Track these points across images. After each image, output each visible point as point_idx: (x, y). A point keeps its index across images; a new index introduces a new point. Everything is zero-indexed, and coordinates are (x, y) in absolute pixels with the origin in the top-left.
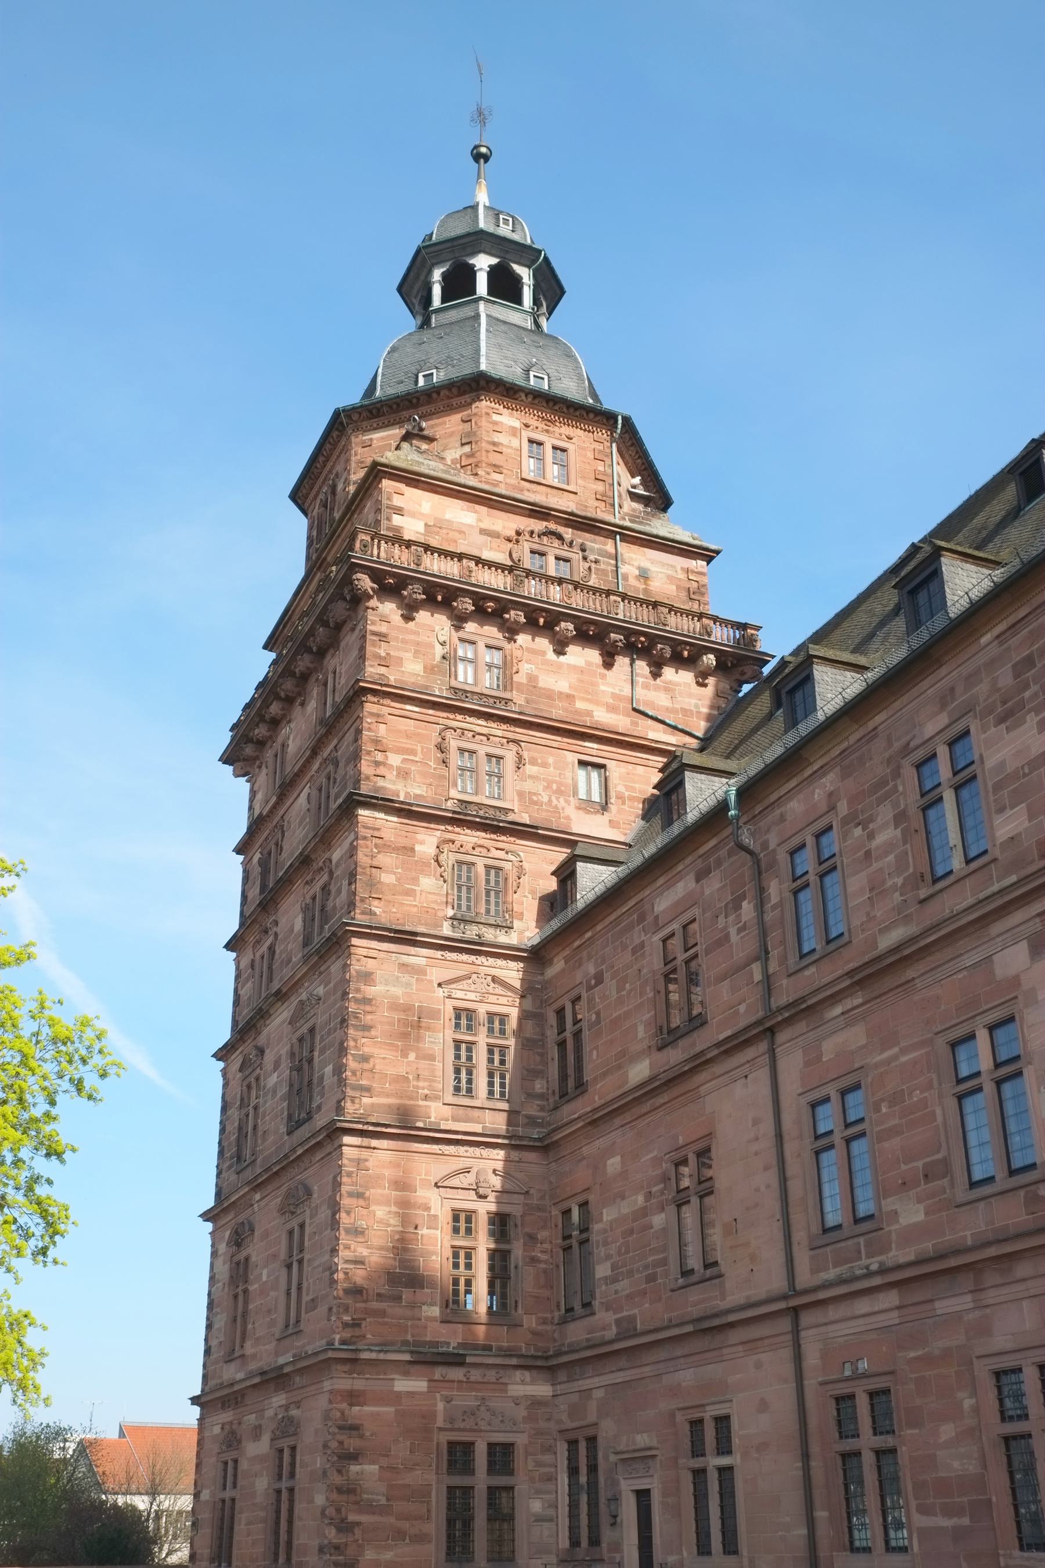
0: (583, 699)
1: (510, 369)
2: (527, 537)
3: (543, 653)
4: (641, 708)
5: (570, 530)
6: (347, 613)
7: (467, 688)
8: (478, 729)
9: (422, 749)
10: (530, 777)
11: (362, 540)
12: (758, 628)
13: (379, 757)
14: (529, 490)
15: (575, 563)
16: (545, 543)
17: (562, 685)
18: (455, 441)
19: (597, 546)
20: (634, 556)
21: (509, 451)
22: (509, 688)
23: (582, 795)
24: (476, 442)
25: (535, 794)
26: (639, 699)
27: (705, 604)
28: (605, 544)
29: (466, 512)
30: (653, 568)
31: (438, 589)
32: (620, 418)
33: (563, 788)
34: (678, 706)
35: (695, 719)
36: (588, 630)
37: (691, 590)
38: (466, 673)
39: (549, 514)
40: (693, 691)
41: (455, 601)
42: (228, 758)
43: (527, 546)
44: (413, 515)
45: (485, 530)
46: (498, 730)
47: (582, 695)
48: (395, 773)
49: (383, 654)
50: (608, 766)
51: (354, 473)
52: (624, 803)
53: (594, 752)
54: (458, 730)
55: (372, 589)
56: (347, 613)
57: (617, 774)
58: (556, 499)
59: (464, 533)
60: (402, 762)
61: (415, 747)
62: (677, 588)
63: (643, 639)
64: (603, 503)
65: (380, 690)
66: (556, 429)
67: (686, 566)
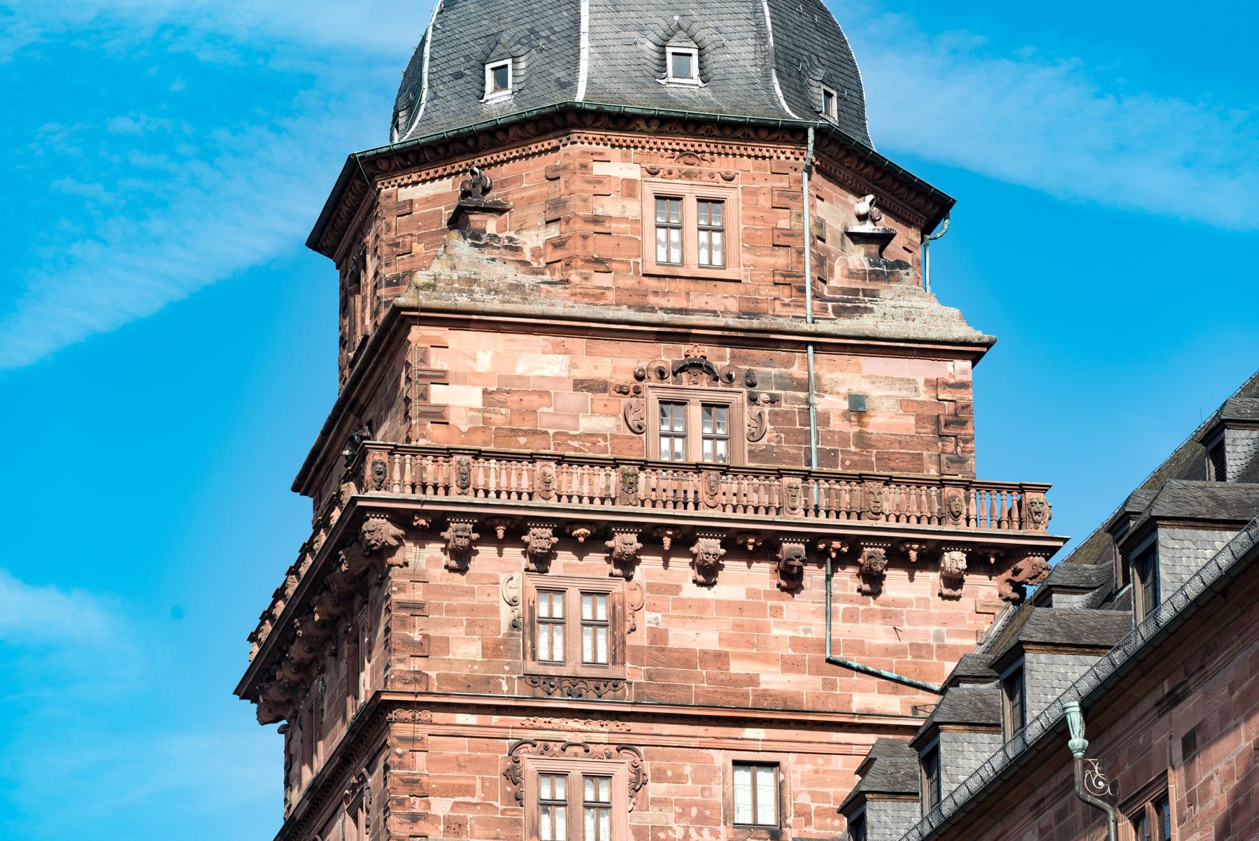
0: (743, 657)
1: (632, 48)
2: (654, 381)
3: (677, 589)
4: (840, 657)
5: (728, 350)
6: (367, 562)
7: (551, 671)
8: (568, 737)
9: (483, 783)
10: (654, 801)
11: (374, 464)
12: (1044, 489)
13: (418, 806)
14: (656, 293)
15: (734, 409)
16: (685, 385)
17: (705, 638)
18: (536, 215)
19: (774, 371)
20: (837, 375)
21: (623, 226)
22: (619, 660)
23: (744, 817)
24: (568, 222)
25: (662, 829)
26: (838, 641)
27: (966, 441)
28: (789, 364)
29: (551, 356)
30: (874, 392)
31: (497, 522)
32: (811, 131)
33: (708, 813)
34: (906, 642)
35: (935, 660)
36: (746, 543)
37: (942, 419)
38: (551, 643)
39: (691, 334)
40: (932, 611)
41: (526, 533)
42: (247, 690)
43: (652, 398)
44: (463, 380)
45: (582, 381)
46: (601, 732)
47: (739, 650)
48: (442, 828)
49: (418, 638)
50: (784, 764)
51: (387, 265)
52: (808, 823)
53: (760, 746)
54: (538, 743)
55: (396, 537)
56: (367, 562)
57: (798, 776)
58: (705, 299)
59: (548, 393)
60: (452, 809)
61: (472, 782)
62: (917, 421)
63: (836, 544)
64: (786, 290)
65: (413, 702)
66: (705, 167)
67: (933, 377)
